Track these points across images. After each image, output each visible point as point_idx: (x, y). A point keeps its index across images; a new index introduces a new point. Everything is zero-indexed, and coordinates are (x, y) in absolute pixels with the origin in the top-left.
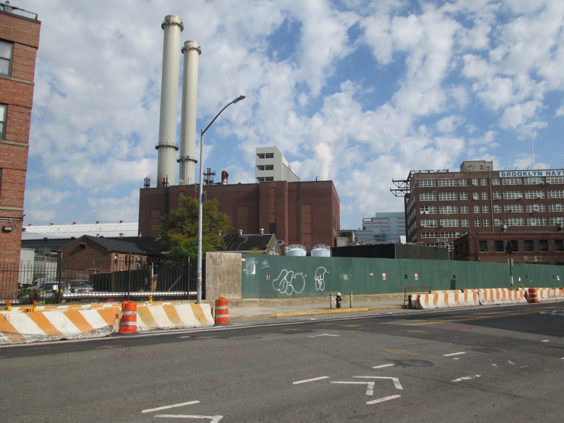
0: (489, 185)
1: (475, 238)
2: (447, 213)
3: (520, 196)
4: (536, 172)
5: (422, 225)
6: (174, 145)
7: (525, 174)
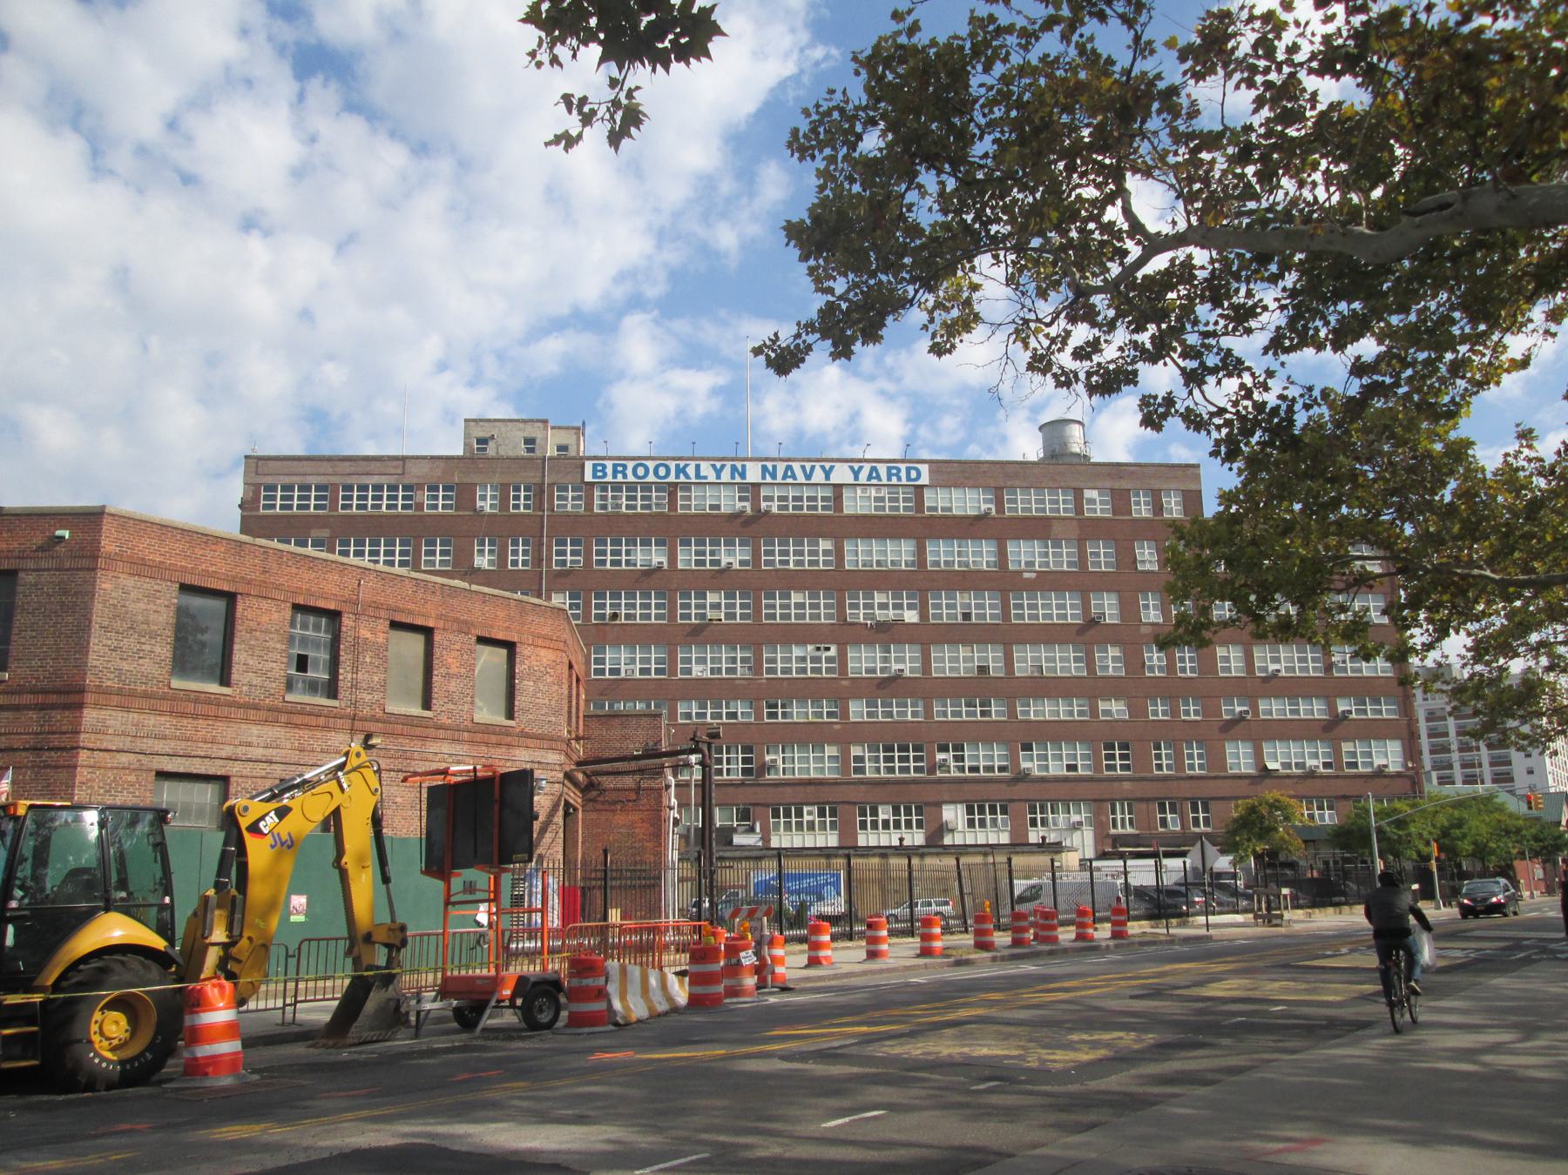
3: (658, 557)
4: (723, 466)
7: (680, 471)
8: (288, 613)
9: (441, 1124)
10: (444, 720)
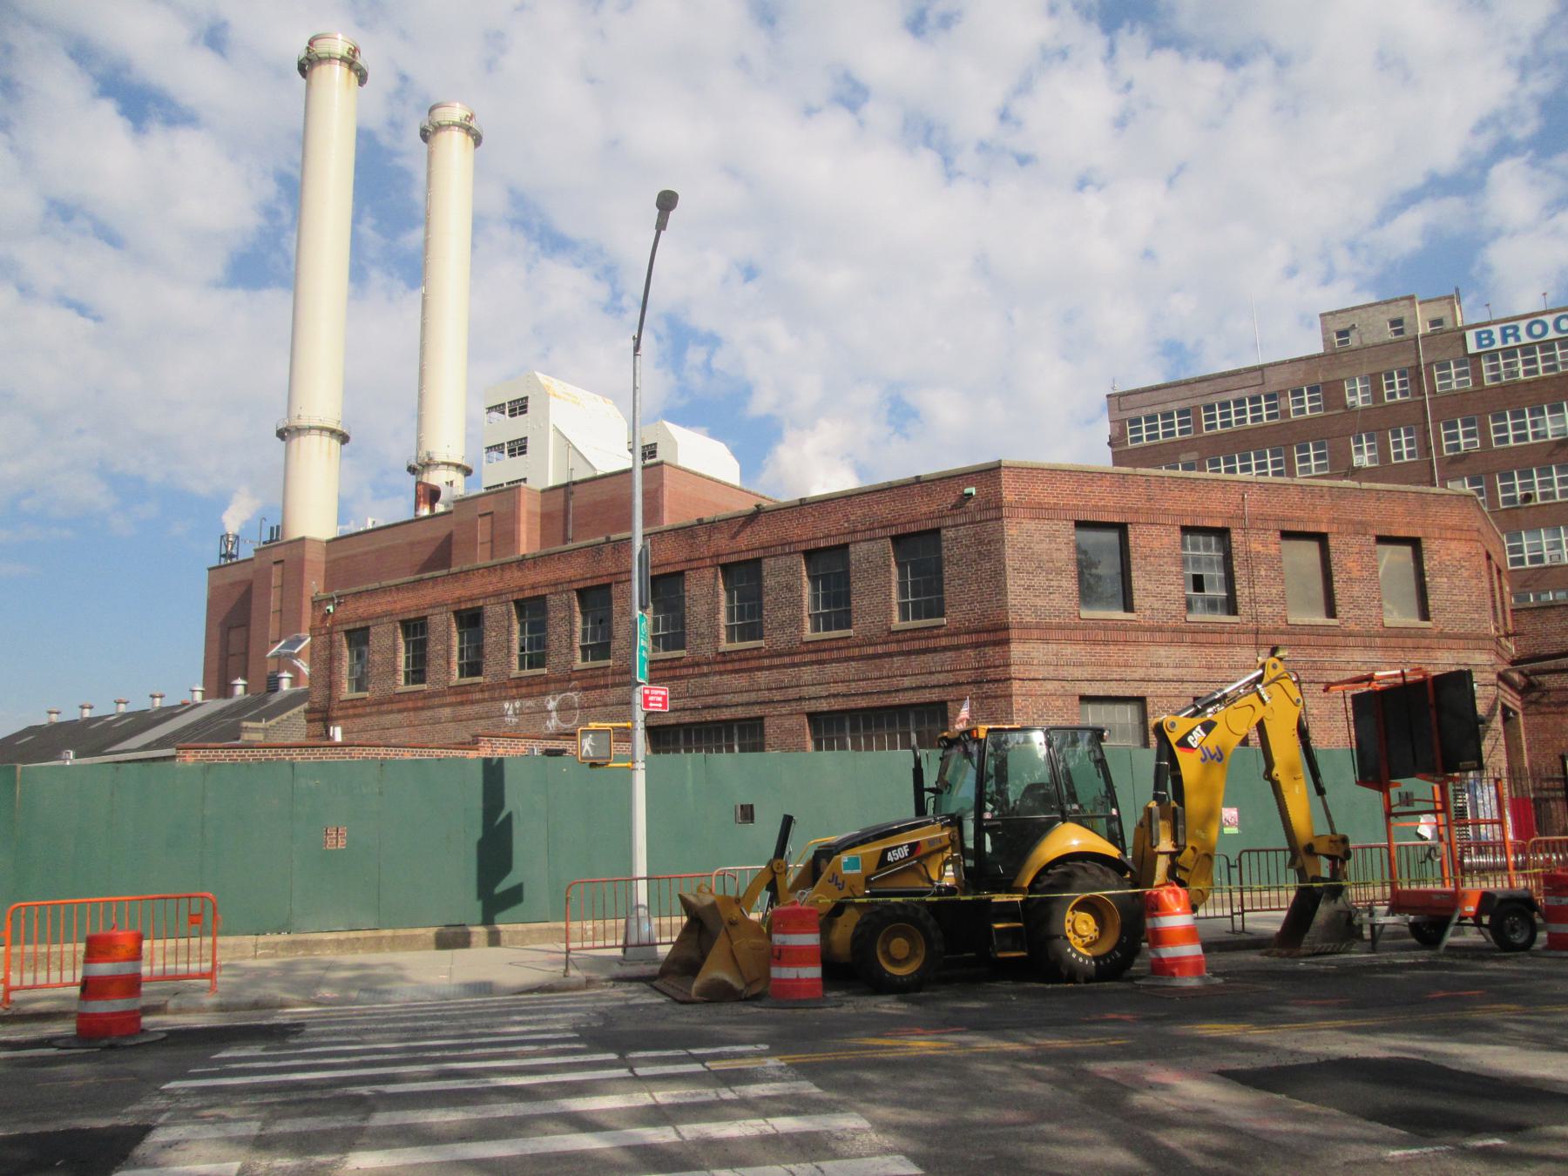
0: (1420, 398)
6: (333, 426)
8: (1177, 535)
9: (1431, 1041)
10: (1352, 626)
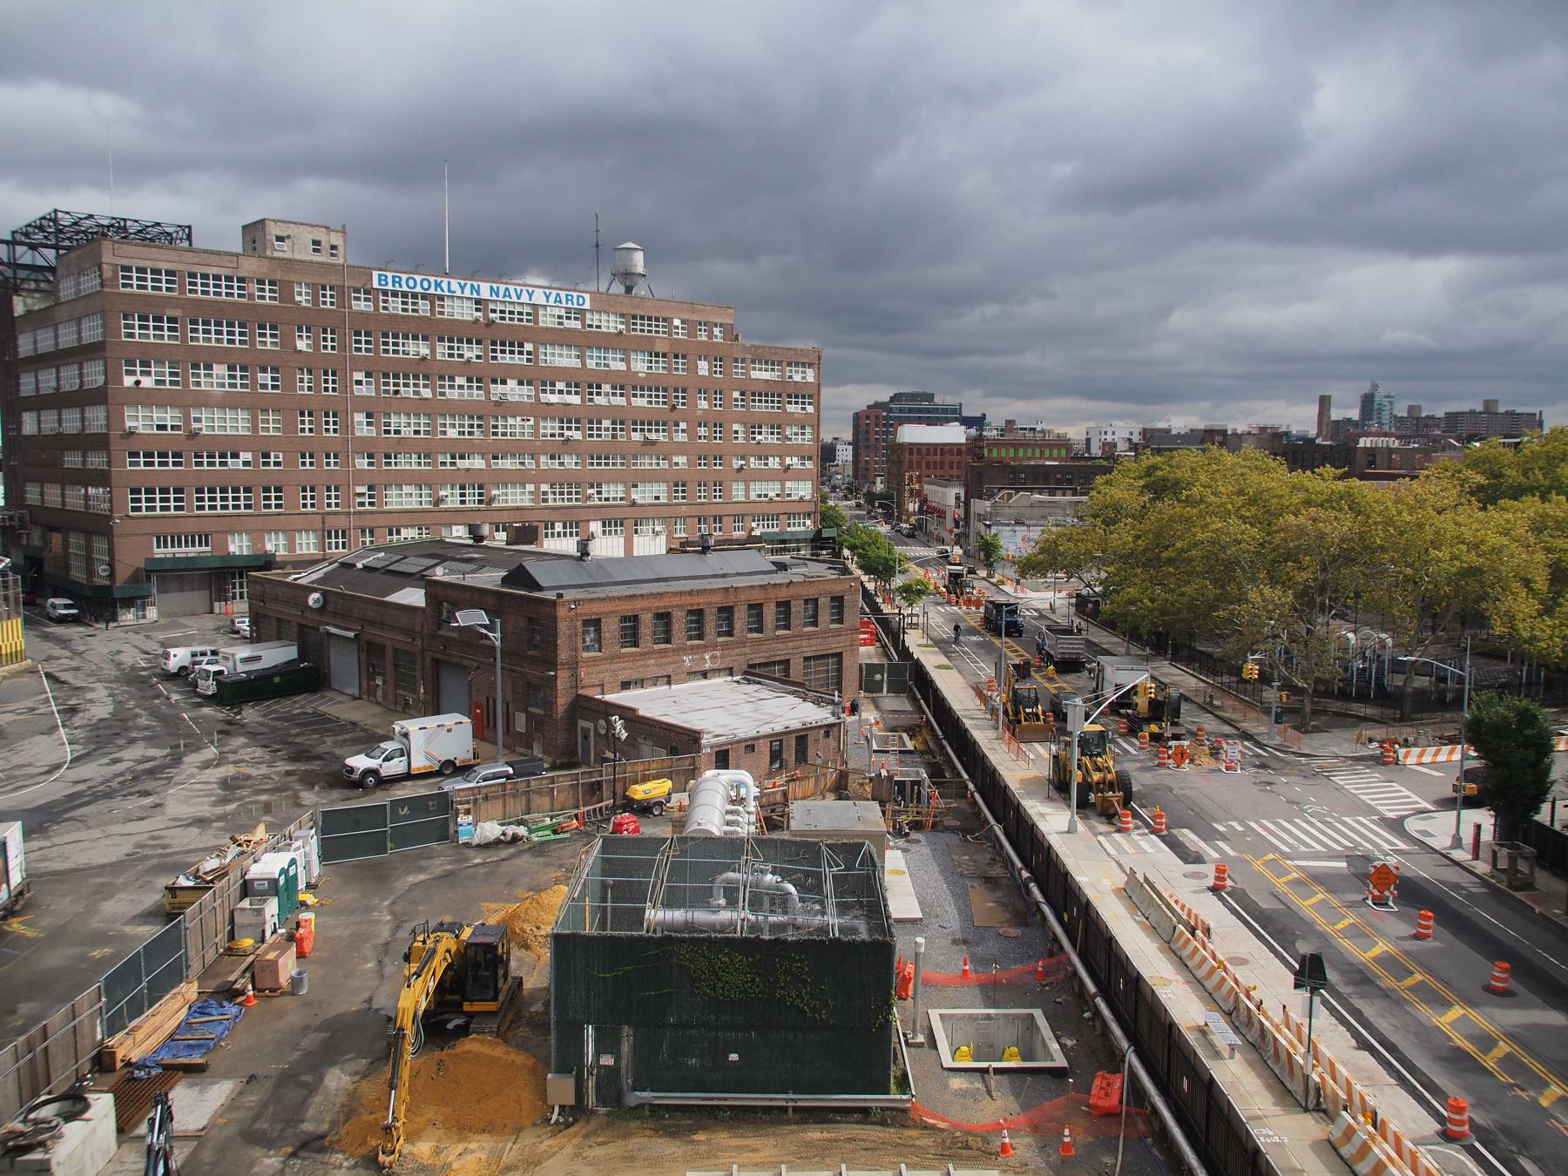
1: (572, 613)
2: (215, 388)
5: (129, 424)
